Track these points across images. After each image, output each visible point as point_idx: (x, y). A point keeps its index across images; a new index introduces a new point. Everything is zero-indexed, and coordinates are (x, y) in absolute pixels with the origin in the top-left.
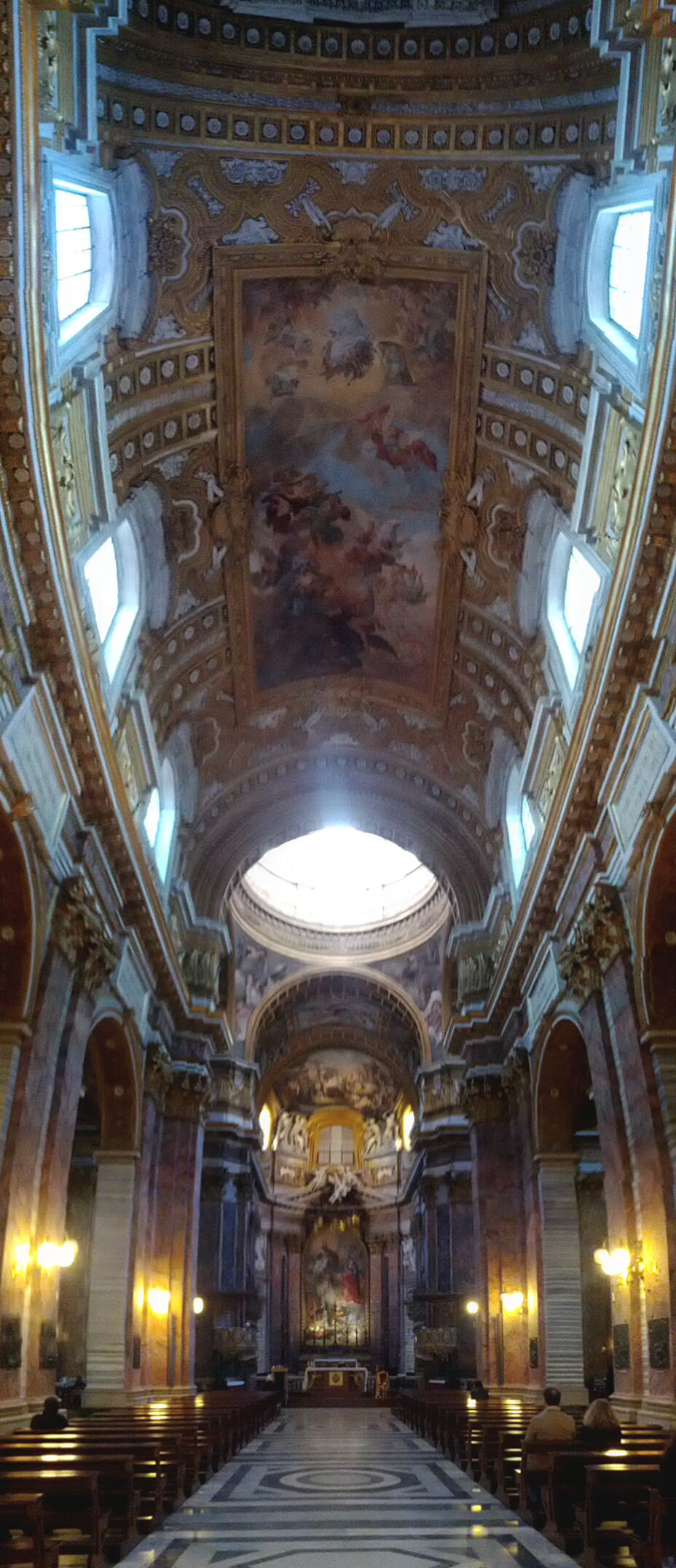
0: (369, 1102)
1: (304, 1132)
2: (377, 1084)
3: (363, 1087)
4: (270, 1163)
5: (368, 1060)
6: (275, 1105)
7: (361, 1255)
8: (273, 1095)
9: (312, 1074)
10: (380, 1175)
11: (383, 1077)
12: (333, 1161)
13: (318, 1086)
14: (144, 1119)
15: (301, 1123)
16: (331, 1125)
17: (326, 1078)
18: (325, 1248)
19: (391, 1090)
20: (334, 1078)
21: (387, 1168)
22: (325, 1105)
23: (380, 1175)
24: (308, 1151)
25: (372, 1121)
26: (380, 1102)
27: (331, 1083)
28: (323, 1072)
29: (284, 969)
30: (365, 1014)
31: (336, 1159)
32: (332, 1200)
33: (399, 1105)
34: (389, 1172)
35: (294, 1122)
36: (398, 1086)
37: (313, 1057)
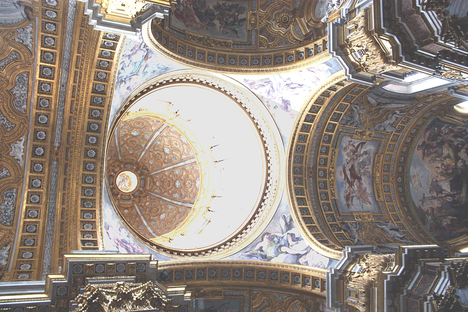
0: (463, 150)
2: (442, 143)
3: (449, 156)
5: (418, 153)
9: (436, 204)
11: (433, 138)
13: (449, 199)
17: (441, 191)
20: (440, 184)
26: (460, 139)
27: (446, 187)
28: (435, 194)
29: (284, 217)
30: (354, 152)
33: (457, 120)
37: (418, 203)
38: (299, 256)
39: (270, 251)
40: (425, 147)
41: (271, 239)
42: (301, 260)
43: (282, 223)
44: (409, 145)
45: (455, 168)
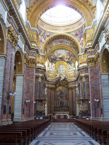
0: (68, 60)
1: (54, 67)
2: (70, 56)
3: (67, 57)
4: (47, 73)
5: (68, 52)
6: (48, 61)
7: (67, 91)
8: (48, 59)
9: (56, 55)
10: (71, 75)
11: (71, 55)
12: (61, 72)
13: (57, 57)
14: (24, 68)
15: (54, 65)
16: (60, 65)
17: (59, 55)
18: (59, 90)
19: (73, 57)
20: (61, 55)
21: (72, 73)
22: (59, 61)
23: (71, 75)
24: (55, 70)
25: (69, 64)
27: (60, 56)
29: (49, 35)
31: (61, 72)
32: (61, 80)
34: (73, 74)
35: (52, 64)
36: (74, 57)
37: (56, 51)
38: (41, 41)
39: (41, 34)
40: (69, 53)
41: (44, 33)
42: (41, 42)
43: (48, 34)
44: (70, 51)
45: (64, 58)
